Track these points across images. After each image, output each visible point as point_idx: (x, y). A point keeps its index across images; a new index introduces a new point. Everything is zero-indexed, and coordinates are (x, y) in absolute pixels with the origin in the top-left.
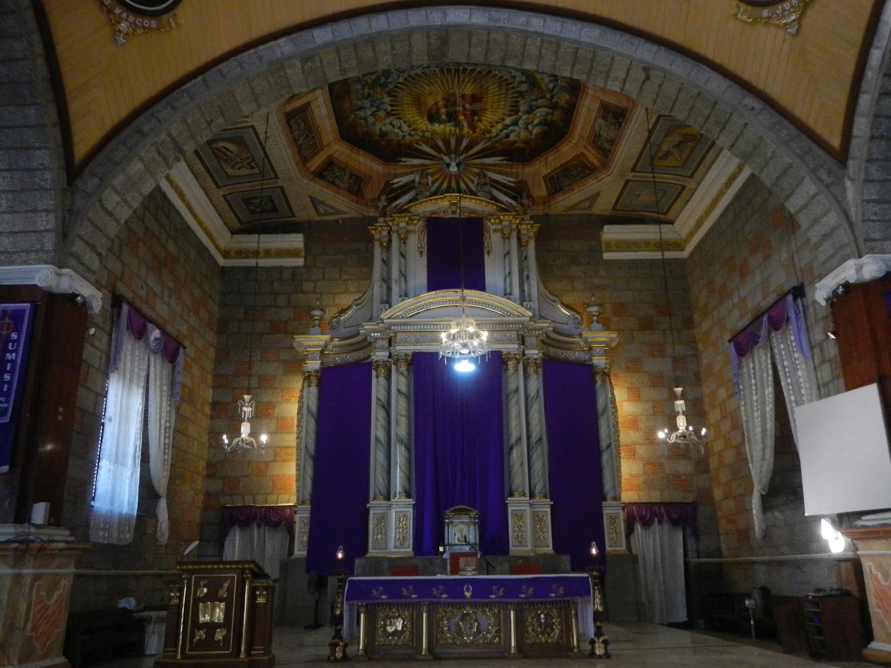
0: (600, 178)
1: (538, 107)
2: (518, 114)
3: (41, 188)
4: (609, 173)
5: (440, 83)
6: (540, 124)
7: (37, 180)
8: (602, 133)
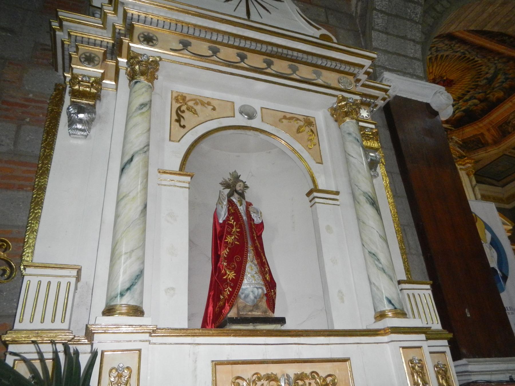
0: (487, 151)
1: (475, 98)
2: (459, 101)
3: (411, 20)
4: (496, 148)
5: (444, 67)
6: (464, 111)
7: (409, 11)
8: (512, 121)
